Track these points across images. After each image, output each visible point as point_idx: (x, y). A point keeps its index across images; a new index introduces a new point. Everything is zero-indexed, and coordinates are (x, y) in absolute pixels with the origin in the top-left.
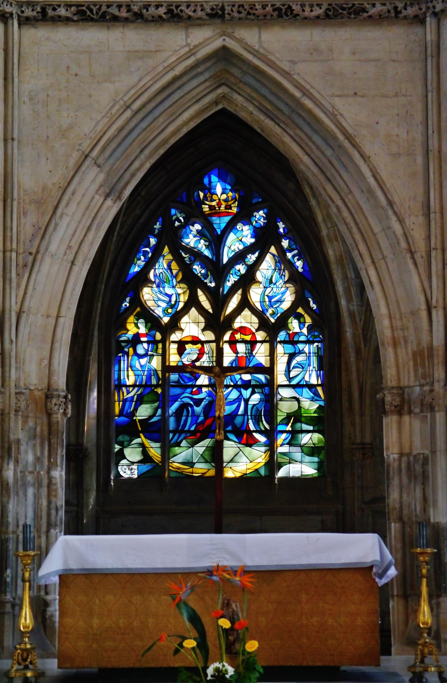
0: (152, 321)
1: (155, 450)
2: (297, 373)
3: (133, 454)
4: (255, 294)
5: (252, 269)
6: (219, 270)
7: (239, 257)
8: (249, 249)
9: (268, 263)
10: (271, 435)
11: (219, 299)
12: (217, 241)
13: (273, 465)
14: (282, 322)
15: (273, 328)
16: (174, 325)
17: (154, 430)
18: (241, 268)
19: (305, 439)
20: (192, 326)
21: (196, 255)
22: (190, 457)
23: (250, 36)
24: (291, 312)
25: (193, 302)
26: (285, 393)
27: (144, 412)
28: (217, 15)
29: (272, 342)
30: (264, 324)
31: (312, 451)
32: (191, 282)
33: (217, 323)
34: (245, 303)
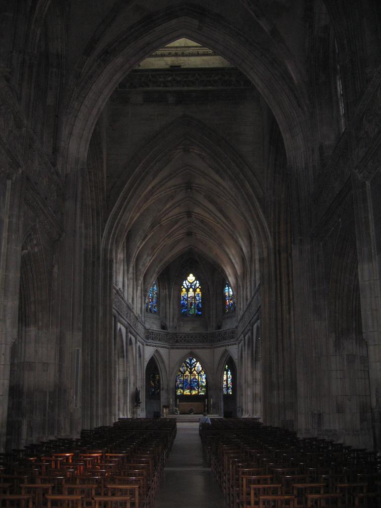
0: (182, 372)
1: (182, 391)
2: (203, 380)
3: (179, 391)
4: (196, 368)
5: (196, 365)
6: (191, 365)
7: (194, 363)
8: (195, 362)
9: (198, 363)
10: (198, 389)
11: (191, 369)
12: (191, 361)
13: (199, 393)
14: (200, 373)
15: (199, 373)
16: (185, 373)
17: (182, 388)
18: (194, 365)
19: (203, 389)
20: (187, 373)
21: (188, 363)
22: (187, 392)
23: (195, 350)
24: (201, 371)
25: (187, 370)
26: (200, 383)
27: (180, 386)
28: (191, 348)
29: (198, 376)
30: (197, 373)
31: (204, 391)
32: (187, 367)
33: (191, 373)
34: (195, 370)
